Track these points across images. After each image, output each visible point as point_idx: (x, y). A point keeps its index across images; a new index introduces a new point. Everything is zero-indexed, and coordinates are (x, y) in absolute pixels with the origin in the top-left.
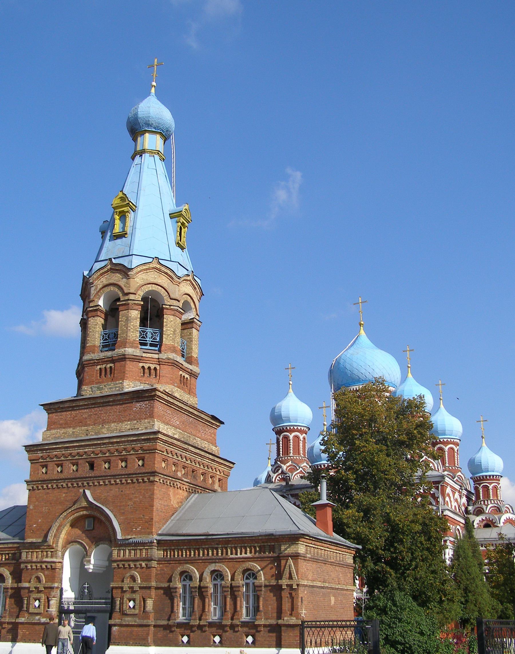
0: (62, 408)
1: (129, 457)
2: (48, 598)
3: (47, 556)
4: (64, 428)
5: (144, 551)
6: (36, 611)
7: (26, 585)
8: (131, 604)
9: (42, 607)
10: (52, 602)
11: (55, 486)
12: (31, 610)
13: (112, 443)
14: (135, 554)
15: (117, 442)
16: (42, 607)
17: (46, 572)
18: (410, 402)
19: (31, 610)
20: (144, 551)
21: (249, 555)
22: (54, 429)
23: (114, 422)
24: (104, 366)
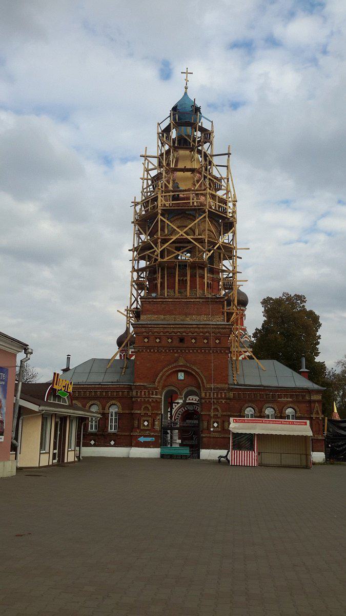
0: (155, 302)
1: (198, 337)
2: (154, 420)
3: (152, 394)
4: (157, 314)
5: (223, 394)
6: (146, 428)
7: (139, 412)
8: (146, 423)
9: (150, 426)
10: (156, 423)
11: (156, 351)
12: (142, 427)
13: (198, 328)
14: (217, 395)
15: (202, 328)
16: (150, 426)
17: (152, 404)
18: (267, 312)
19: (142, 427)
20: (223, 394)
21: (289, 400)
22: (149, 314)
23: (194, 315)
24: (182, 278)
